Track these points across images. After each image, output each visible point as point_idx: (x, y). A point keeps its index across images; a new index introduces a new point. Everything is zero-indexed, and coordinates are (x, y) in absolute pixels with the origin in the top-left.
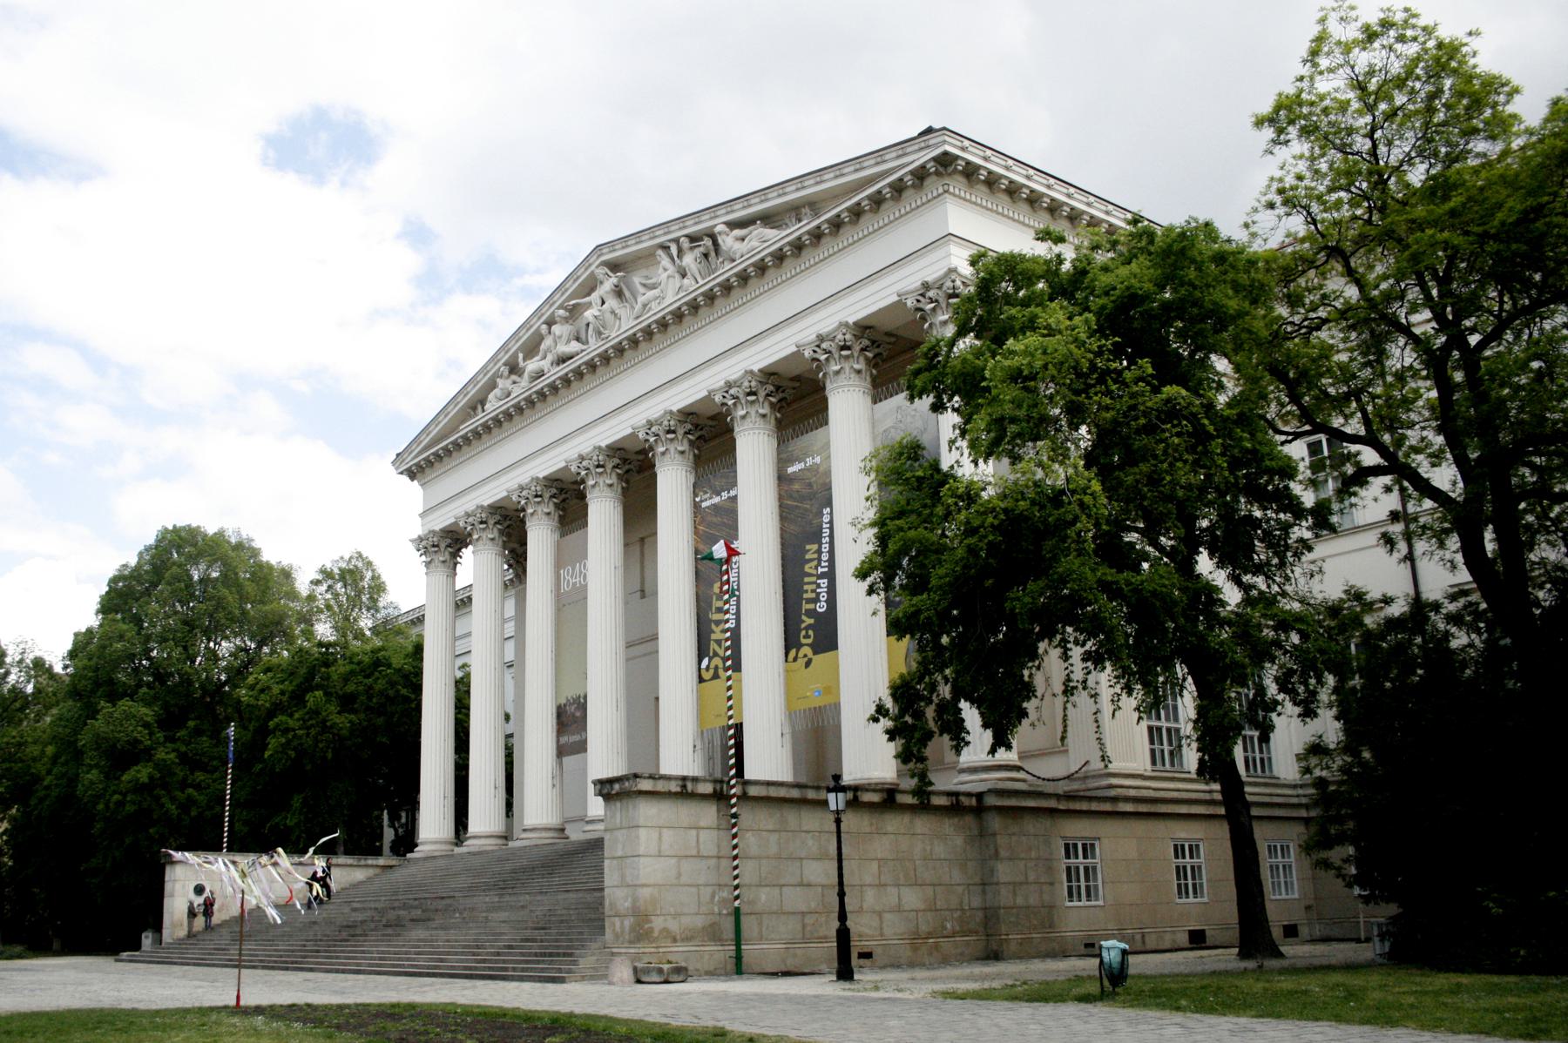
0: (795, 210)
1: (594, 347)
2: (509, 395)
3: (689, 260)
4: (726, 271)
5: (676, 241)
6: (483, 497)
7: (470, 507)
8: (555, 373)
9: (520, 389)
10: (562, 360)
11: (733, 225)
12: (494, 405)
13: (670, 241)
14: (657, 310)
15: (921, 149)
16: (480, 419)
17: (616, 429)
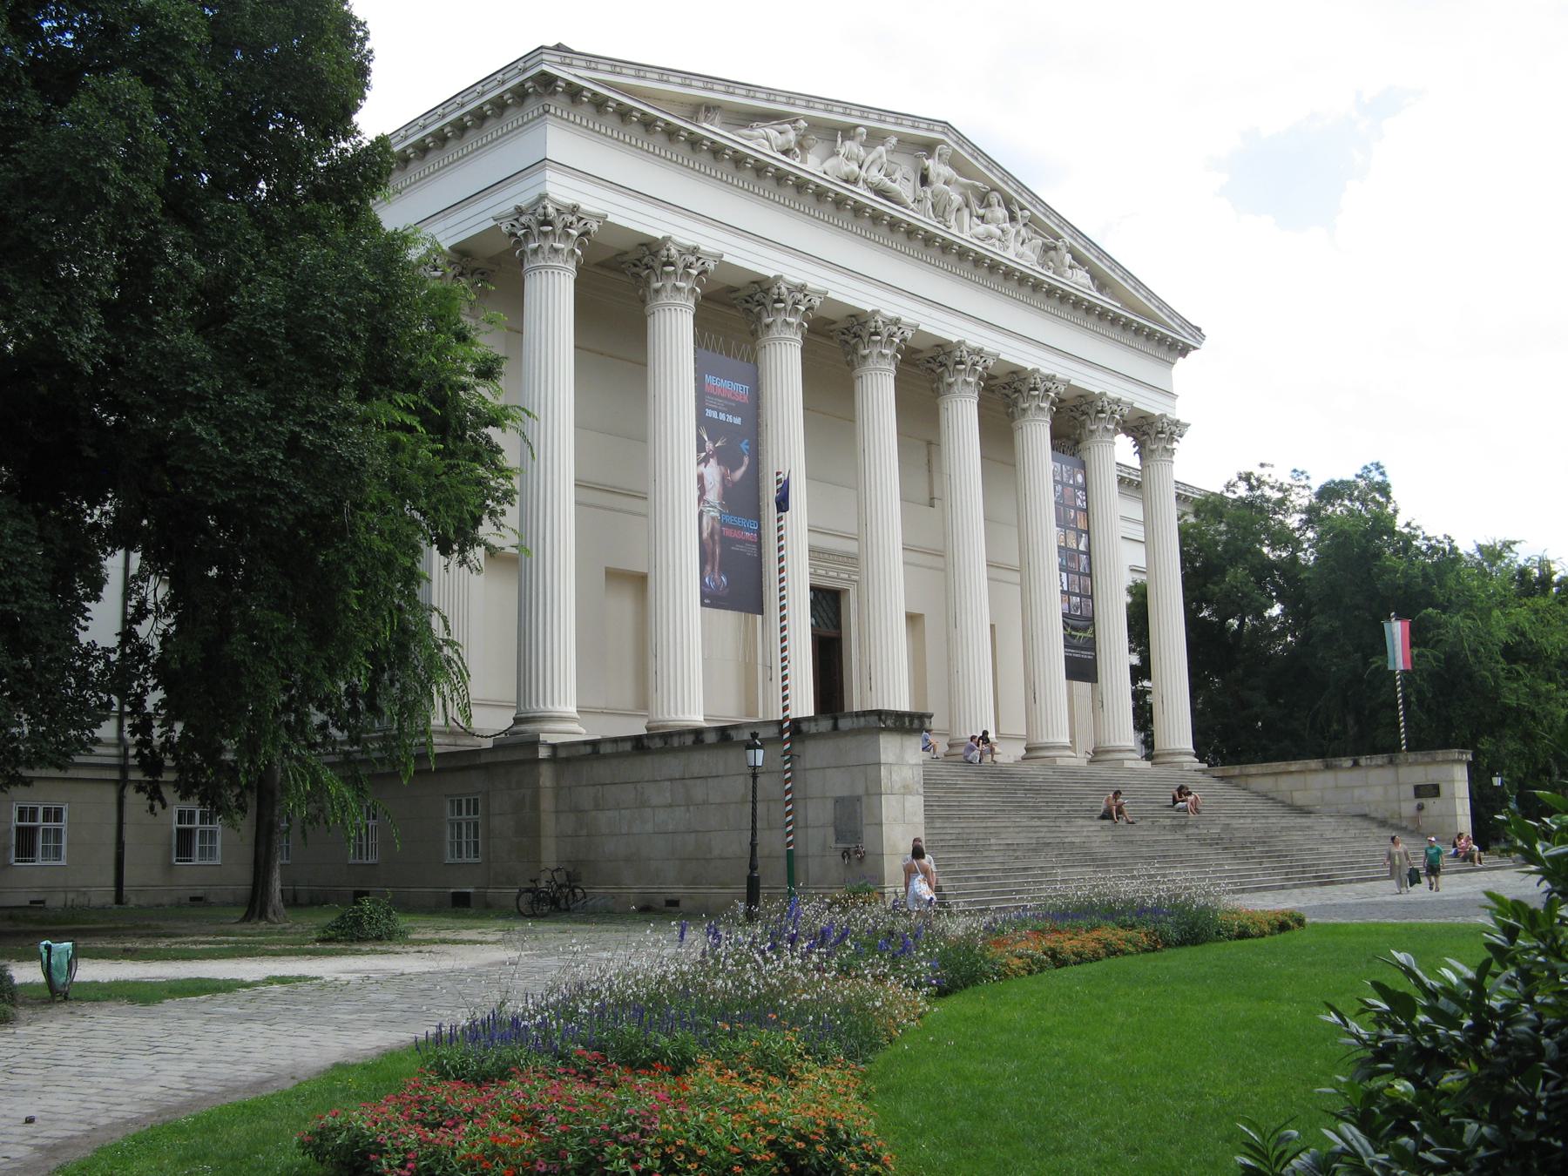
0: (1101, 282)
1: (926, 220)
2: (786, 152)
3: (1023, 231)
4: (1047, 275)
5: (1022, 208)
6: (1141, 399)
7: (989, 347)
8: (863, 194)
9: (813, 165)
10: (881, 192)
11: (1071, 250)
12: (762, 143)
13: (1016, 200)
14: (993, 250)
15: (1190, 335)
16: (712, 129)
17: (1091, 381)
